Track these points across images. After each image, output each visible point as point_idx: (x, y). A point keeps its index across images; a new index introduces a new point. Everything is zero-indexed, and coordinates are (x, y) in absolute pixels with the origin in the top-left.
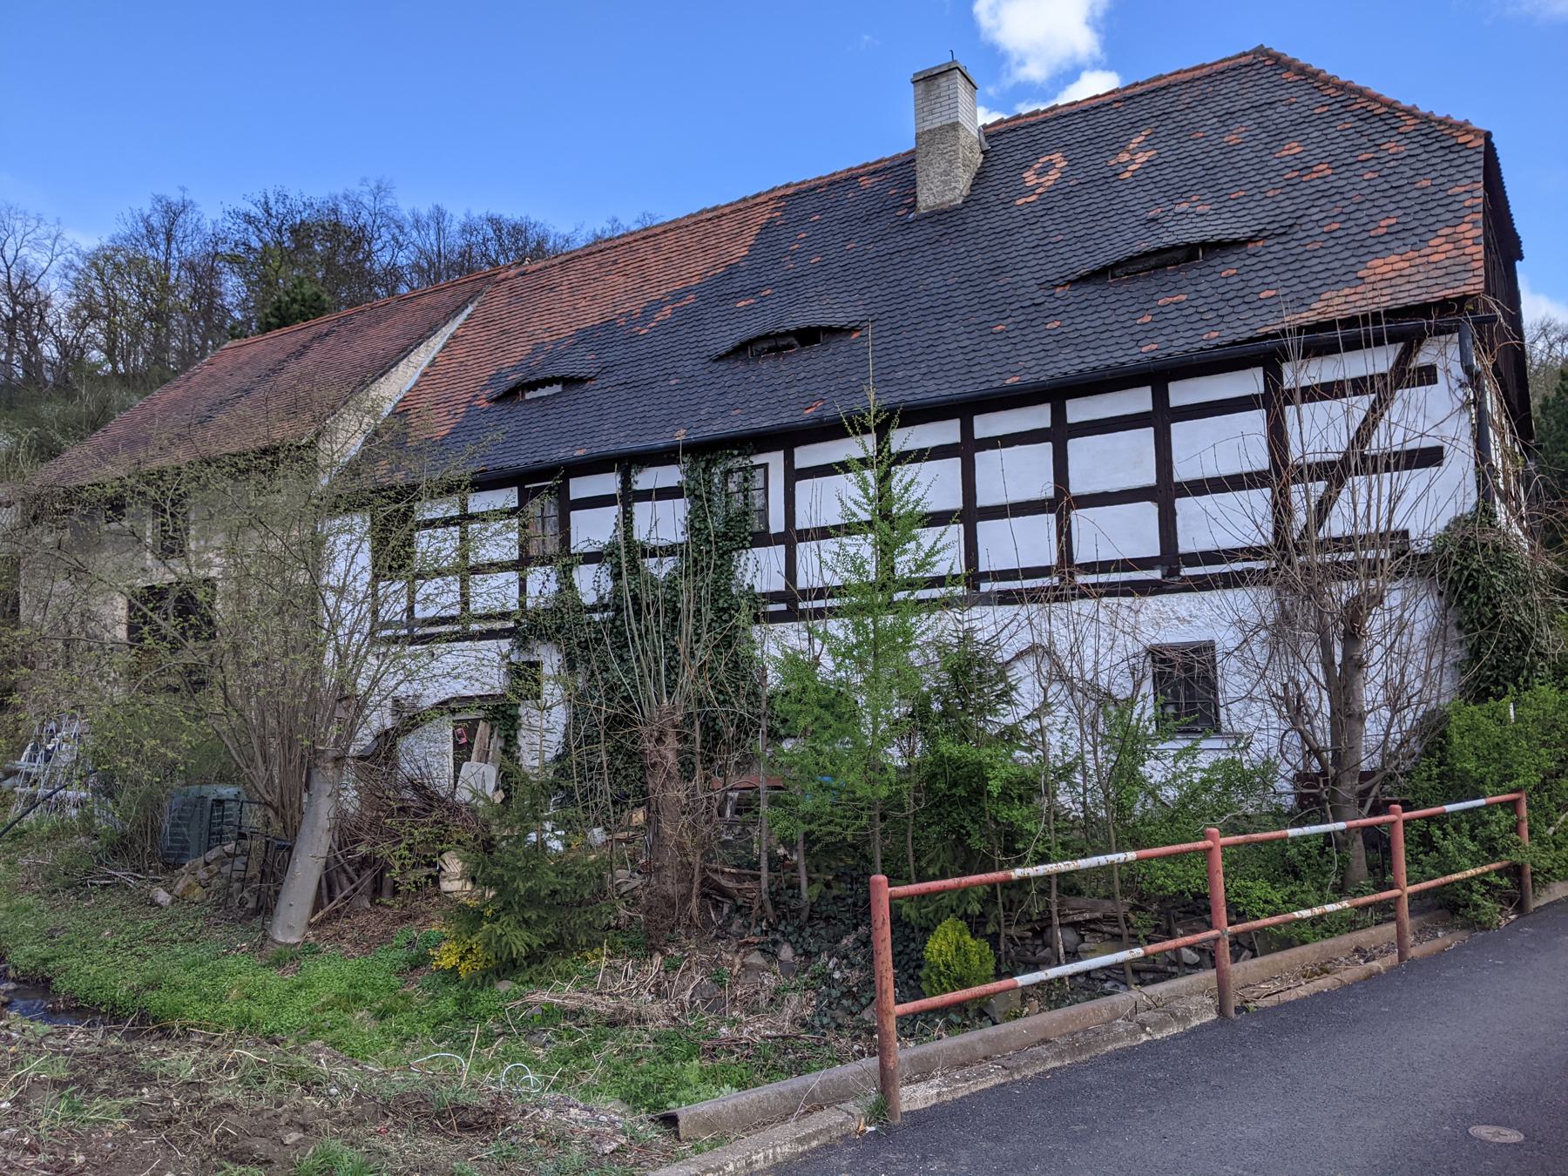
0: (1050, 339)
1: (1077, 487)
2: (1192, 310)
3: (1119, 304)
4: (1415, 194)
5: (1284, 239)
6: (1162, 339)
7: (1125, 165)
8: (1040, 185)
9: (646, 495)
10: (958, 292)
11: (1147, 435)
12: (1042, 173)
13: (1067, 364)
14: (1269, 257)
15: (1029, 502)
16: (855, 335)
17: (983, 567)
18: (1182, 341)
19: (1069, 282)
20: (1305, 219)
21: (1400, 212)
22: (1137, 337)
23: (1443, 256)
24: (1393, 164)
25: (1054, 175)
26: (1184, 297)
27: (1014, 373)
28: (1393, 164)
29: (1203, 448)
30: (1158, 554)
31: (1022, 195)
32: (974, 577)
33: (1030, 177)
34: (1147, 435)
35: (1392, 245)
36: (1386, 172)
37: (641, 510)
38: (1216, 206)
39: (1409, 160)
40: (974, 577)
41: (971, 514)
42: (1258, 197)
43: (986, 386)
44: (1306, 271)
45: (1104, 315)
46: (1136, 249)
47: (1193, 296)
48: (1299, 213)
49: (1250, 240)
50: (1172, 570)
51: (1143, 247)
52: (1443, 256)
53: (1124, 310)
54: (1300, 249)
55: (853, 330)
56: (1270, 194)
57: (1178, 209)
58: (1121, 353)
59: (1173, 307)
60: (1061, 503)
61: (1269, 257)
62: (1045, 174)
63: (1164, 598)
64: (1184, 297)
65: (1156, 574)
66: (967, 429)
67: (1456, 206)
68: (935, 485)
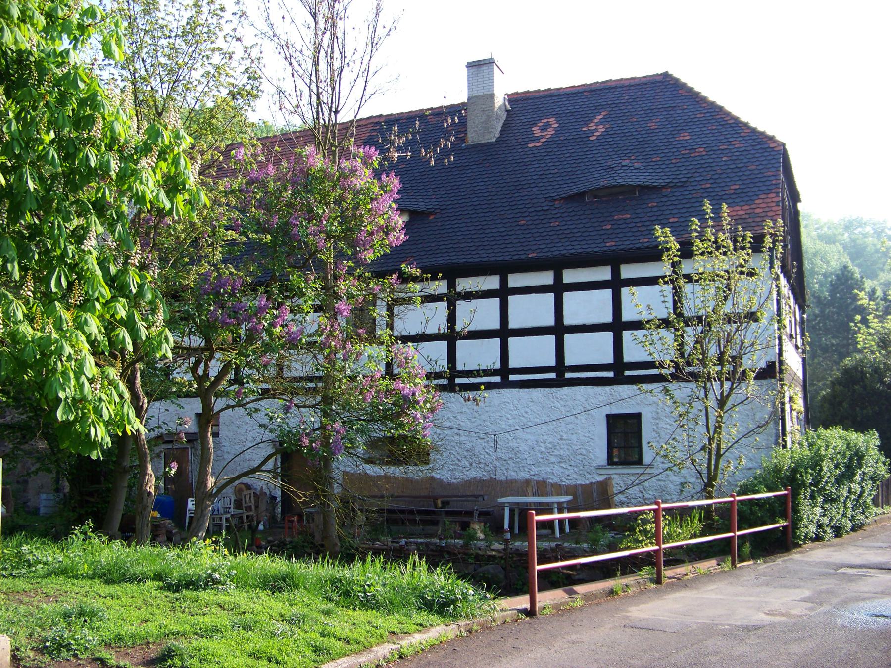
0: (553, 233)
1: (513, 324)
2: (633, 225)
3: (592, 216)
4: (748, 173)
5: (681, 189)
6: (617, 240)
7: (593, 132)
8: (543, 137)
9: (468, 296)
10: (496, 197)
11: (608, 293)
12: (544, 129)
13: (564, 249)
14: (674, 198)
15: (584, 325)
16: (431, 217)
17: (460, 367)
18: (628, 243)
19: (563, 198)
20: (693, 179)
21: (740, 182)
22: (603, 237)
23: (761, 210)
24: (737, 154)
25: (550, 132)
26: (628, 216)
27: (533, 251)
28: (737, 154)
29: (639, 303)
30: (612, 362)
31: (532, 141)
32: (505, 370)
33: (536, 131)
34: (608, 293)
35: (736, 201)
36: (734, 158)
37: (462, 307)
38: (644, 164)
39: (744, 153)
40: (560, 366)
41: (504, 333)
42: (667, 162)
43: (486, 259)
44: (693, 209)
45: (584, 221)
46: (602, 184)
47: (634, 216)
48: (689, 175)
49: (664, 187)
50: (619, 372)
51: (605, 183)
52: (761, 210)
53: (595, 220)
54: (690, 196)
55: (431, 213)
56: (674, 161)
57: (624, 163)
58: (579, 247)
59: (622, 221)
60: (559, 330)
61: (674, 198)
62: (545, 131)
63: (615, 388)
64: (628, 216)
65: (611, 374)
66: (504, 282)
67: (767, 183)
68: (485, 314)
